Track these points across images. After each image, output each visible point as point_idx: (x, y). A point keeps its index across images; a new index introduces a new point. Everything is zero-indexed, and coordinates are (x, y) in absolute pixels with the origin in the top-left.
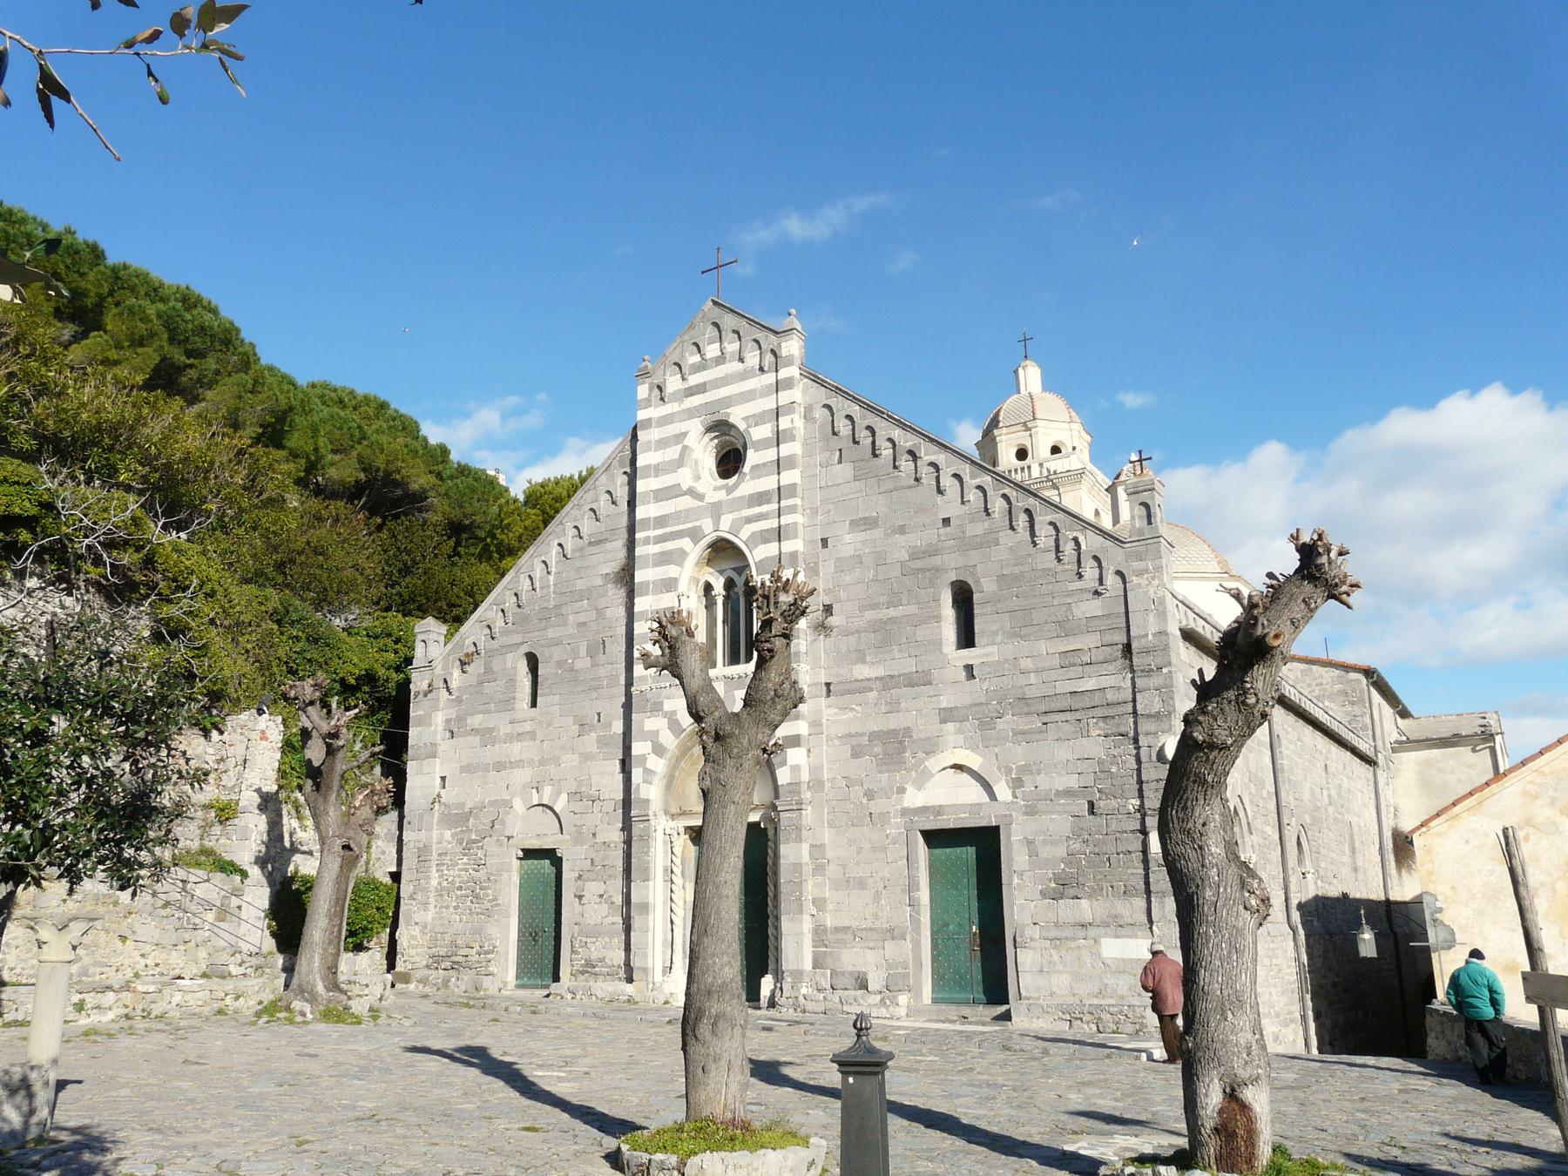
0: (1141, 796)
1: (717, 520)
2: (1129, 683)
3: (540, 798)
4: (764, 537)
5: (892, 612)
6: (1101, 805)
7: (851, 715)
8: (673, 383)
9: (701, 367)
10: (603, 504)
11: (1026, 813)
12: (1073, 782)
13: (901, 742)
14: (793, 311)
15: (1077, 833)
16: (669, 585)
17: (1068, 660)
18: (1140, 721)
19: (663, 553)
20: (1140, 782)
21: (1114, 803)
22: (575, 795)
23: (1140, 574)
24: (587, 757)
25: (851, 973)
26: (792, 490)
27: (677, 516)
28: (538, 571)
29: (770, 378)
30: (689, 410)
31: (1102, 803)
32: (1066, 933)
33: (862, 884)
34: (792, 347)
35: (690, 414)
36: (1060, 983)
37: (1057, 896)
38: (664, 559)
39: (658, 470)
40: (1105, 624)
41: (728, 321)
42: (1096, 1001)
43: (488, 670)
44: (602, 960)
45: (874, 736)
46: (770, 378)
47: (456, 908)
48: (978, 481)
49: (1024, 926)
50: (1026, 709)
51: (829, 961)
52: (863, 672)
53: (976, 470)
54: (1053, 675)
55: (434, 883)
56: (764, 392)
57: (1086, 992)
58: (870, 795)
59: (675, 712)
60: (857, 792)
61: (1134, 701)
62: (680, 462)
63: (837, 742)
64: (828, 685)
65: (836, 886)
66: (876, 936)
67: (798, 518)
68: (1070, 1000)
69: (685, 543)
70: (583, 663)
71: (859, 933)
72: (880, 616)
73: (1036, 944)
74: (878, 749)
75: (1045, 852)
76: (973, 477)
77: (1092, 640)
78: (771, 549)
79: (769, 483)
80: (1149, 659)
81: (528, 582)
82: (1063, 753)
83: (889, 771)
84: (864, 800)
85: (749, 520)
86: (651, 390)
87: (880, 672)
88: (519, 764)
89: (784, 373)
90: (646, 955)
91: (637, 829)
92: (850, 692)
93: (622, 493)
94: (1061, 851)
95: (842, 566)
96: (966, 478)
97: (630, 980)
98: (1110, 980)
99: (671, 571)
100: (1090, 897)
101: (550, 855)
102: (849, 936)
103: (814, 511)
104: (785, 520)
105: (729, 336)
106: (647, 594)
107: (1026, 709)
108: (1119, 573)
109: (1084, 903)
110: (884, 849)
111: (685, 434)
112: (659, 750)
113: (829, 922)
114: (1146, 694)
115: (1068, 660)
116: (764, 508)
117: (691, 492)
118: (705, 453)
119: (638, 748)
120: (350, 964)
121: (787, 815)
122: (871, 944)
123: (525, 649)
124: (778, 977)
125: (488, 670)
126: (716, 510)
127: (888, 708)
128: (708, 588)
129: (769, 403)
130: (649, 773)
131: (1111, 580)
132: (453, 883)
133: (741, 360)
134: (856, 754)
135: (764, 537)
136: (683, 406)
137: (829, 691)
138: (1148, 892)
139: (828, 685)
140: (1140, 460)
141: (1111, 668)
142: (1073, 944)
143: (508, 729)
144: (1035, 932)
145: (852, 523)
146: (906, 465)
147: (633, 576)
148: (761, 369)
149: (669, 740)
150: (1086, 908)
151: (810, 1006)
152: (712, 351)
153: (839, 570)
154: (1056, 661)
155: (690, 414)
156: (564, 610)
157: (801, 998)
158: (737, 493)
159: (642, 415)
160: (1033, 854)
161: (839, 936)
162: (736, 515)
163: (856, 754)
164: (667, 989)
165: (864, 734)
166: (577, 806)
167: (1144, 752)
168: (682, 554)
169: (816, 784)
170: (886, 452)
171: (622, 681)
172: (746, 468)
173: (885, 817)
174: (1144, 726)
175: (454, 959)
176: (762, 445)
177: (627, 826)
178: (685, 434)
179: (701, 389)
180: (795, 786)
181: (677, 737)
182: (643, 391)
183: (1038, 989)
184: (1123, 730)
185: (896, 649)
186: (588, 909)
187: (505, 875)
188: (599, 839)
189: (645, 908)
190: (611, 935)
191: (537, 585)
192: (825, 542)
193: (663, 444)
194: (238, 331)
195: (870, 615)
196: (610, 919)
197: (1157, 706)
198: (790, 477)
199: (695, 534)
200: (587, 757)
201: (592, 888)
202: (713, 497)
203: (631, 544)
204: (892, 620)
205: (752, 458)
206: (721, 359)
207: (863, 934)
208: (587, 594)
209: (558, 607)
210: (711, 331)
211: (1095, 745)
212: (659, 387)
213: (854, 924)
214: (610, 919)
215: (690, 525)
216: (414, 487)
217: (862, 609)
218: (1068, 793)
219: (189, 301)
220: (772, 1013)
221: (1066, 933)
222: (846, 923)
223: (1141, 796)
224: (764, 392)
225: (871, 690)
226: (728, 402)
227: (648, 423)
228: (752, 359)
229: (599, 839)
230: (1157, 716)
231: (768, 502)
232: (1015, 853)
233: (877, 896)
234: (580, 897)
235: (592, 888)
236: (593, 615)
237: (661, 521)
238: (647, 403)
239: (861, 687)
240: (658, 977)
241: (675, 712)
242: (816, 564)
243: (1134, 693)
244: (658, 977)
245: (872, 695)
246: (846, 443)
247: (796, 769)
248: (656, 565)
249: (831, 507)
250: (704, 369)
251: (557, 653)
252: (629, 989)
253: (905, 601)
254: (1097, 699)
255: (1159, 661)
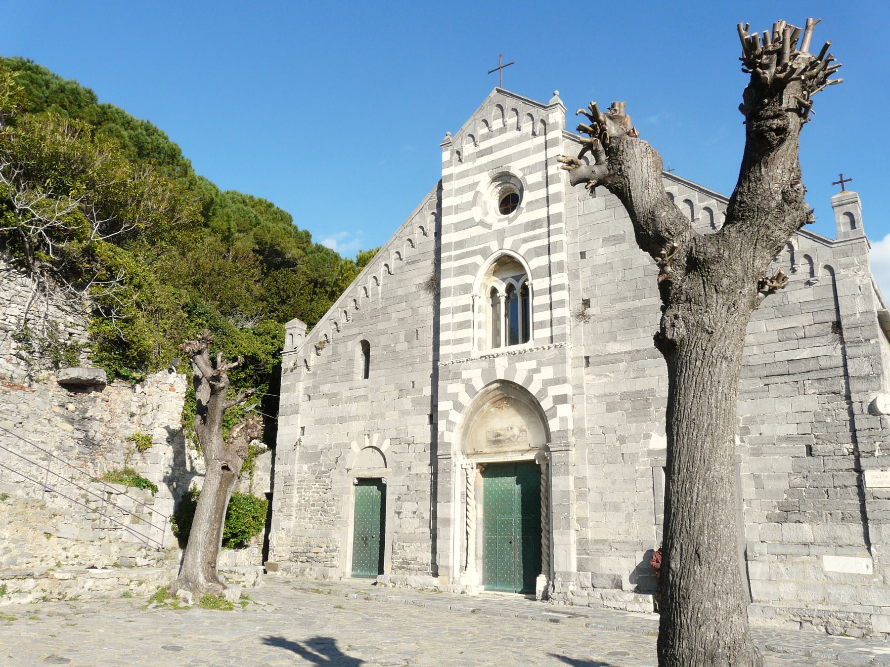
0: (854, 440)
1: (501, 241)
2: (839, 352)
3: (371, 442)
4: (537, 252)
5: (637, 303)
6: (818, 448)
7: (605, 380)
8: (468, 149)
10: (417, 236)
11: (753, 455)
12: (793, 430)
13: (647, 400)
14: (557, 92)
15: (797, 471)
16: (466, 289)
17: (784, 335)
18: (851, 381)
19: (461, 267)
20: (853, 430)
21: (830, 447)
22: (396, 440)
23: (846, 267)
24: (404, 413)
25: (608, 576)
26: (559, 217)
27: (472, 240)
28: (371, 284)
29: (541, 140)
30: (480, 166)
31: (819, 447)
32: (790, 550)
33: (616, 507)
34: (557, 116)
35: (481, 169)
36: (788, 590)
37: (781, 521)
38: (462, 271)
39: (457, 209)
40: (817, 307)
41: (509, 103)
42: (820, 607)
43: (335, 353)
44: (415, 559)
45: (624, 396)
46: (541, 140)
47: (310, 519)
48: (705, 204)
49: (753, 543)
50: (750, 374)
51: (591, 566)
52: (614, 347)
53: (703, 196)
54: (773, 347)
55: (296, 501)
56: (536, 150)
57: (812, 599)
58: (622, 440)
59: (470, 380)
60: (612, 438)
61: (845, 366)
62: (474, 203)
63: (595, 401)
64: (587, 358)
65: (595, 508)
66: (628, 547)
67: (562, 237)
68: (797, 605)
69: (478, 259)
70: (402, 346)
71: (614, 545)
72: (627, 306)
73: (765, 558)
74: (628, 405)
75: (770, 485)
76: (700, 201)
77: (806, 320)
78: (543, 260)
79: (541, 213)
80: (856, 333)
81: (363, 291)
82: (783, 407)
83: (636, 422)
84: (618, 444)
85: (526, 241)
86: (452, 154)
87: (628, 347)
88: (356, 418)
89: (550, 136)
90: (447, 557)
91: (441, 464)
92: (604, 363)
93: (431, 228)
94: (784, 485)
95: (596, 271)
96: (696, 202)
97: (436, 574)
98: (833, 590)
99: (467, 279)
100: (811, 522)
101: (377, 482)
102: (607, 547)
103: (575, 232)
104: (553, 239)
105: (509, 113)
106: (449, 295)
107: (750, 374)
108: (828, 268)
109: (805, 525)
110: (634, 481)
111: (477, 184)
112: (458, 407)
113: (590, 535)
114: (857, 361)
115: (784, 335)
116: (537, 232)
117: (482, 223)
118: (491, 196)
119: (442, 406)
120: (226, 558)
121: (557, 454)
122: (625, 554)
123: (361, 338)
124: (551, 576)
125: (335, 353)
126: (501, 235)
127: (636, 374)
128: (494, 291)
130: (450, 423)
131: (820, 272)
132: (308, 501)
133: (519, 129)
134: (610, 409)
135: (537, 252)
136: (476, 164)
137: (588, 363)
138: (865, 519)
139: (587, 358)
140: (841, 182)
141: (823, 340)
142: (798, 559)
143: (348, 394)
144: (764, 548)
145: (604, 240)
147: (439, 284)
148: (534, 134)
149: (466, 400)
150: (807, 531)
151: (576, 600)
152: (496, 124)
153: (595, 274)
154: (775, 336)
155: (481, 169)
156: (389, 310)
157: (569, 594)
158: (516, 222)
159: (445, 172)
160: (759, 486)
161: (598, 546)
162: (516, 237)
163: (610, 409)
164: (464, 582)
165: (616, 394)
166: (397, 448)
167: (856, 407)
168: (476, 266)
169: (579, 431)
171: (431, 358)
172: (523, 204)
173: (634, 457)
174: (855, 386)
175: (308, 554)
176: (535, 187)
177: (434, 462)
178: (477, 184)
179: (489, 151)
180: (563, 433)
181: (472, 397)
182: (446, 155)
183: (768, 594)
184: (836, 389)
185: (641, 330)
186: (405, 523)
187: (345, 497)
188: (413, 472)
189: (447, 522)
190: (421, 541)
191: (370, 293)
192: (583, 255)
193: (461, 191)
194: (180, 151)
195: (619, 306)
196: (421, 530)
197: (866, 369)
198: (555, 209)
199: (485, 253)
200: (404, 413)
201: (408, 507)
202: (497, 226)
203: (438, 262)
204: (638, 309)
205: (527, 197)
207: (618, 546)
208: (406, 298)
209: (384, 308)
210: (496, 111)
211: (811, 401)
212: (458, 153)
213: (610, 538)
214: (421, 530)
215: (481, 246)
216: (288, 256)
217: (613, 302)
218: (788, 438)
219: (149, 130)
220: (546, 604)
221: (790, 550)
222: (604, 537)
223: (854, 440)
225: (622, 361)
227: (450, 177)
228: (527, 127)
229: (413, 472)
230: (867, 377)
231: (540, 227)
232: (743, 485)
233: (629, 517)
234: (399, 513)
235: (408, 507)
236: (410, 312)
237: (460, 244)
238: (450, 163)
239: (613, 359)
240: (457, 573)
241: (470, 380)
242: (577, 270)
243: (845, 360)
244: (457, 573)
245: (623, 365)
247: (564, 420)
248: (455, 275)
249: (587, 229)
250: (491, 137)
251: (384, 340)
252: (435, 581)
253: (647, 295)
254: (812, 365)
255: (867, 334)
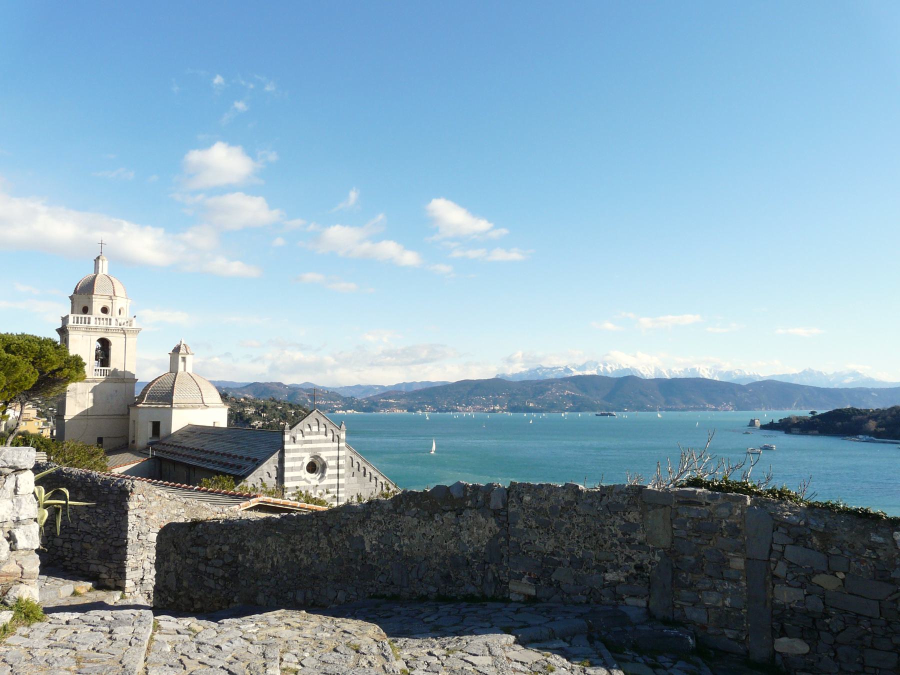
8: (299, 437)
9: (310, 434)
26: (343, 485)
35: (305, 450)
39: (292, 469)
46: (336, 445)
129: (335, 453)
133: (326, 435)
146: (374, 481)
152: (315, 429)
155: (305, 450)
158: (322, 483)
170: (368, 476)
176: (332, 468)
179: (310, 442)
193: (294, 459)
206: (318, 433)
224: (334, 449)
226: (320, 449)
228: (330, 436)
246: (356, 471)
